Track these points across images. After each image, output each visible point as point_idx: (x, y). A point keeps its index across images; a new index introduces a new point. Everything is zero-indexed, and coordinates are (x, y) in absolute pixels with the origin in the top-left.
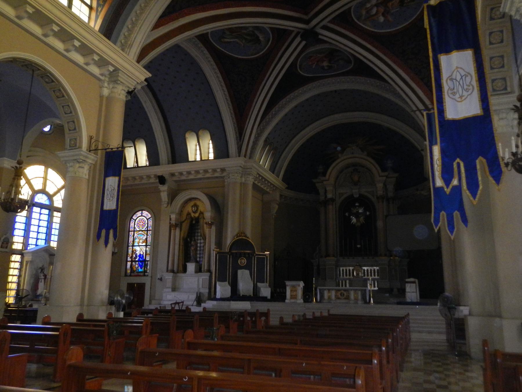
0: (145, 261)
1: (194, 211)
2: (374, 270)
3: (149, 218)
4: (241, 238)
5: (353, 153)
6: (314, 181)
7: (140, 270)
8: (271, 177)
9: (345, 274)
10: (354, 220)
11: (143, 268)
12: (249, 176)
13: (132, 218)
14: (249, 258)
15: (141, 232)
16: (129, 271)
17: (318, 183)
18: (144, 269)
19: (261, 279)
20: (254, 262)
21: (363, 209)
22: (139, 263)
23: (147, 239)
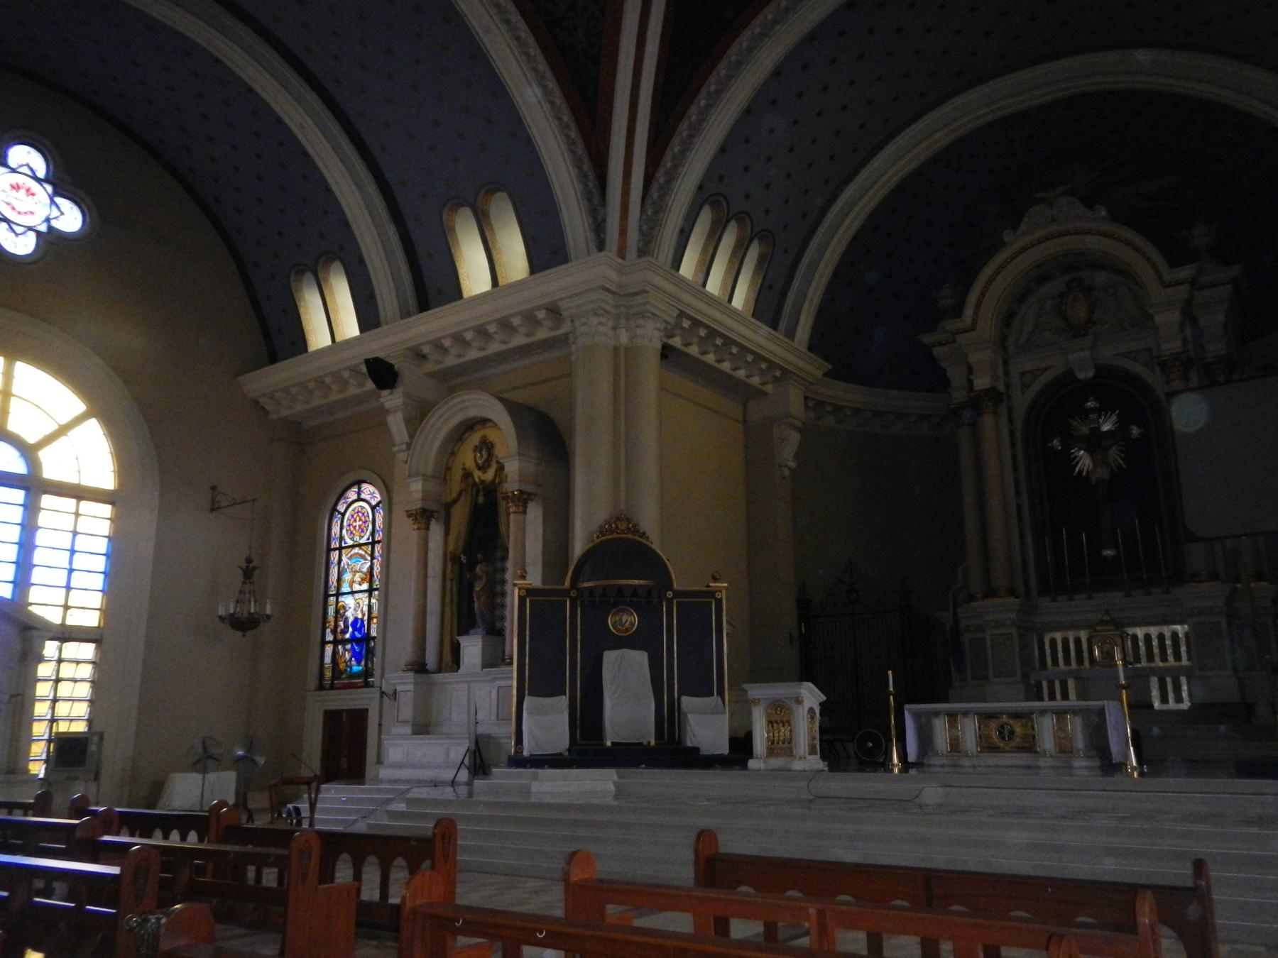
0: (367, 638)
1: (479, 462)
2: (1175, 636)
3: (378, 505)
4: (615, 535)
5: (1053, 220)
6: (927, 339)
7: (356, 668)
8: (760, 337)
9: (1060, 655)
10: (1084, 460)
11: (363, 663)
12: (641, 322)
13: (334, 509)
14: (647, 603)
15: (356, 550)
16: (328, 674)
17: (941, 344)
18: (366, 665)
19: (700, 683)
20: (670, 620)
21: (1114, 418)
22: (352, 646)
23: (371, 567)
